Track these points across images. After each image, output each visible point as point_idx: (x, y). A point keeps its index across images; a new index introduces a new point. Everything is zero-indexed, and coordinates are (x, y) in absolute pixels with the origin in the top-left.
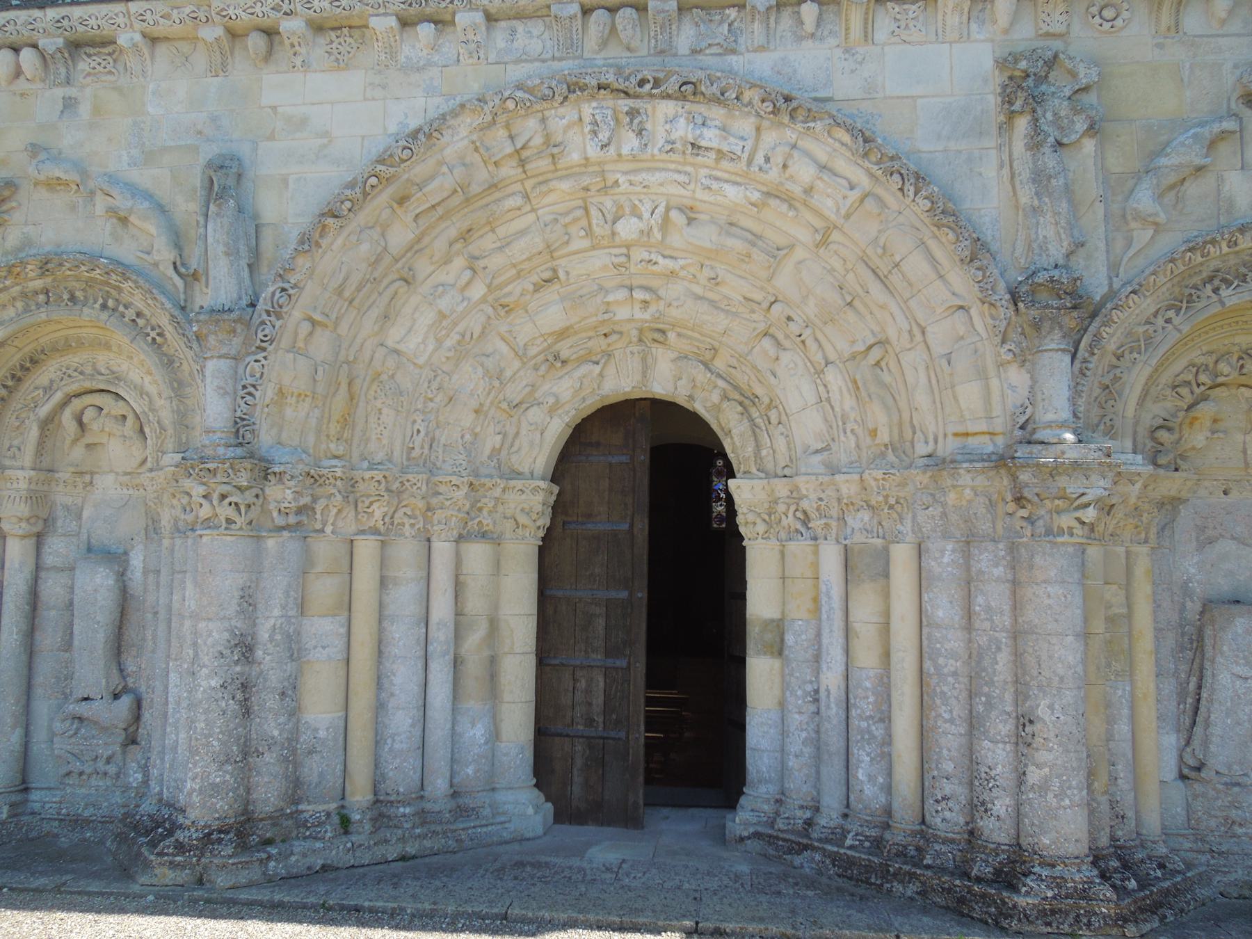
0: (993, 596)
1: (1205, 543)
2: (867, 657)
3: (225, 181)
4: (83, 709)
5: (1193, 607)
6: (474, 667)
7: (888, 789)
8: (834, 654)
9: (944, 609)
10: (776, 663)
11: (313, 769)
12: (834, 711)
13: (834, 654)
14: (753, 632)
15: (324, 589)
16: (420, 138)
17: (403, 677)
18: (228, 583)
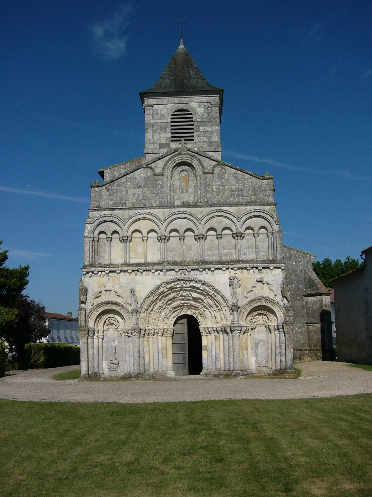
0: (231, 341)
1: (258, 333)
2: (217, 350)
3: (132, 291)
4: (112, 362)
5: (257, 341)
6: (165, 354)
7: (220, 366)
8: (214, 350)
9: (226, 343)
10: (206, 352)
11: (146, 367)
12: (214, 357)
13: (214, 350)
14: (203, 347)
15: (146, 343)
16: (159, 287)
17: (156, 355)
18: (137, 344)
